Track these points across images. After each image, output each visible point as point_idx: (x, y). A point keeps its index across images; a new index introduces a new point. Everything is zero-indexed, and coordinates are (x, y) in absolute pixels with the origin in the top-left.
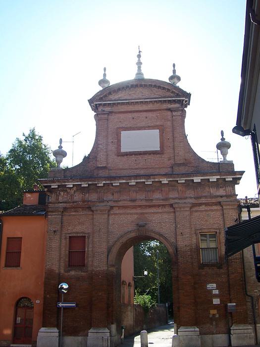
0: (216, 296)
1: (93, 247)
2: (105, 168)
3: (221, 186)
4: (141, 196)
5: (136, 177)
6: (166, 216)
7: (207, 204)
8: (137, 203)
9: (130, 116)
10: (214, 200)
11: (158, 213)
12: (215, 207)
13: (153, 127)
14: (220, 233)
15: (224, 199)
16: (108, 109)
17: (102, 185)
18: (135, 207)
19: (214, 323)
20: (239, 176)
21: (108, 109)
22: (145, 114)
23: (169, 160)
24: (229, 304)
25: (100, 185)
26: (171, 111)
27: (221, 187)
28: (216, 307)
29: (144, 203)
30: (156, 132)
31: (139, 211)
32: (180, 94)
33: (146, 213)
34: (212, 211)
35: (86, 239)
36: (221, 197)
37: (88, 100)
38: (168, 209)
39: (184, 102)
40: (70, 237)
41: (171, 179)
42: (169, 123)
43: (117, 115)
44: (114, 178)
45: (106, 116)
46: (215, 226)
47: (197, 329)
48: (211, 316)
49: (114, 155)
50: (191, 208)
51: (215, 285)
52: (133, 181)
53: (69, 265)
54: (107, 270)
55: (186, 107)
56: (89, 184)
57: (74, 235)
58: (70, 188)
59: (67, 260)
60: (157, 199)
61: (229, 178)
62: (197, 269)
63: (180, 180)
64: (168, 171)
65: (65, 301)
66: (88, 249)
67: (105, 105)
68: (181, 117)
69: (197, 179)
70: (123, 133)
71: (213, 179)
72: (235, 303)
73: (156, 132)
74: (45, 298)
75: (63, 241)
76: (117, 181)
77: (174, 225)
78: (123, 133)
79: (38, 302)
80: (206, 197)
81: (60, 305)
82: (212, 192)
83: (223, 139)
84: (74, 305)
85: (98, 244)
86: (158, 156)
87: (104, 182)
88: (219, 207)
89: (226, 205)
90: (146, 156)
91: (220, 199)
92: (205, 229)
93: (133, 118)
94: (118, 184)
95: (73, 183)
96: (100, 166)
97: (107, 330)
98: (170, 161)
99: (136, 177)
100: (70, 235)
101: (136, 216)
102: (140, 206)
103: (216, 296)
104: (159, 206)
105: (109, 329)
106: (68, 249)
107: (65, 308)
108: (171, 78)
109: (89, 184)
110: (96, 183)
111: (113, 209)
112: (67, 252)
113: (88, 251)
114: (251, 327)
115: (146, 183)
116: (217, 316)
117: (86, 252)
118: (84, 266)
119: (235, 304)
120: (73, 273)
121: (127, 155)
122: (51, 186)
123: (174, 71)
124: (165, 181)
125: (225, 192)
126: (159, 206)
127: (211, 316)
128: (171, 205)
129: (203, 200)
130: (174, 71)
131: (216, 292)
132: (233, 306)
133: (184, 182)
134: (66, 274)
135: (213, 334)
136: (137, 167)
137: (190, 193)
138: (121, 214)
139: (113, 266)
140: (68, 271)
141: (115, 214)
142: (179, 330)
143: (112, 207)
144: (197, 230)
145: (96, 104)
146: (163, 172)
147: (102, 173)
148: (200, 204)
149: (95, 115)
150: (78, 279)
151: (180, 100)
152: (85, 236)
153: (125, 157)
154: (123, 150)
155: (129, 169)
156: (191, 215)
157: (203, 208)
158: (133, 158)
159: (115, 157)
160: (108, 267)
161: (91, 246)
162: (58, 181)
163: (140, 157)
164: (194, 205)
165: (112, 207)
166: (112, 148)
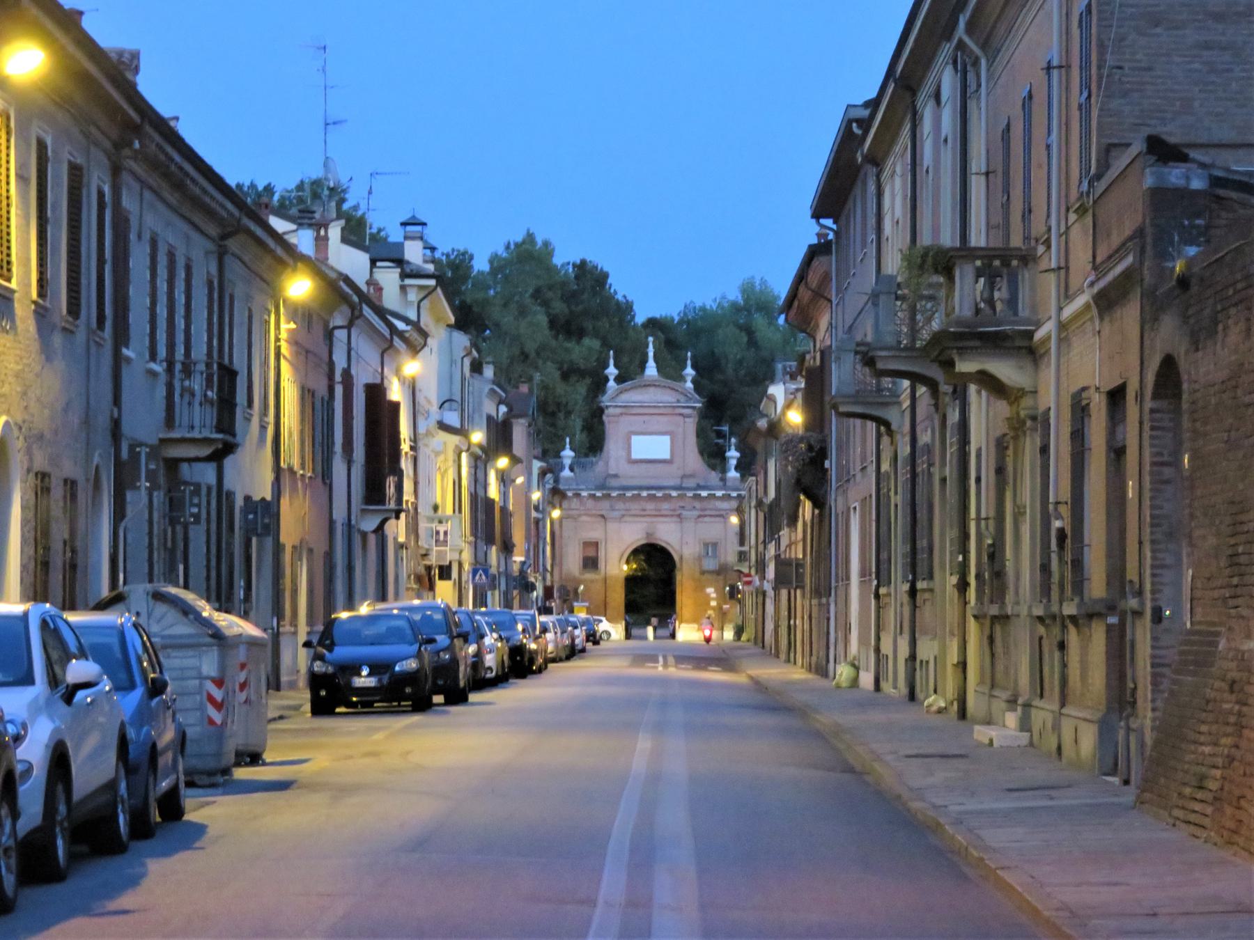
0: (713, 599)
2: (616, 476)
4: (650, 506)
5: (648, 488)
7: (711, 516)
10: (717, 513)
16: (618, 411)
18: (644, 516)
28: (713, 608)
30: (667, 439)
38: (675, 519)
42: (680, 430)
60: (666, 509)
64: (677, 482)
67: (616, 406)
69: (704, 494)
70: (635, 439)
71: (719, 493)
73: (667, 439)
78: (635, 439)
80: (711, 509)
88: (722, 519)
91: (722, 513)
99: (648, 488)
102: (649, 515)
103: (713, 599)
124: (674, 494)
129: (707, 513)
131: (714, 595)
137: (697, 505)
140: (583, 574)
146: (671, 483)
147: (614, 482)
148: (705, 516)
154: (635, 456)
157: (707, 519)
158: (644, 466)
162: (574, 490)
163: (649, 465)
164: (700, 516)
165: (623, 516)
166: (623, 453)
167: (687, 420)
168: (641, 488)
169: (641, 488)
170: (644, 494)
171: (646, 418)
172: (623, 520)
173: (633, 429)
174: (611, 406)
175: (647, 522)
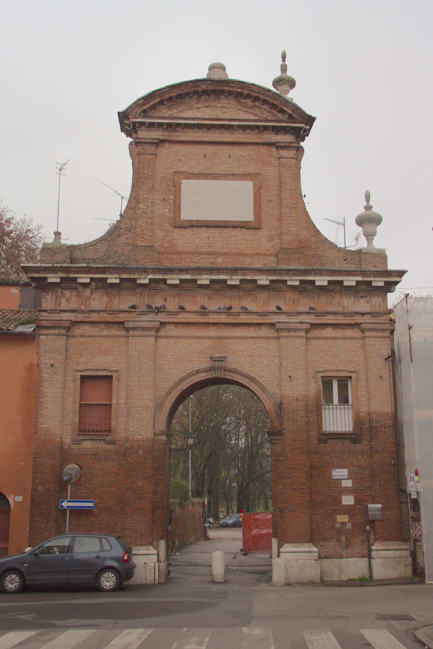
0: (347, 491)
1: (128, 398)
3: (363, 294)
5: (210, 271)
6: (262, 344)
7: (334, 326)
8: (211, 318)
9: (199, 150)
11: (248, 338)
12: (349, 333)
13: (244, 177)
14: (357, 380)
15: (367, 319)
16: (157, 134)
17: (146, 281)
19: (343, 538)
20: (397, 279)
21: (157, 134)
22: (227, 149)
23: (269, 241)
24: (371, 506)
25: (142, 281)
26: (277, 148)
27: (362, 297)
28: (348, 510)
29: (223, 318)
31: (213, 332)
32: (295, 116)
33: (227, 338)
34: (345, 338)
35: (114, 382)
36: (363, 314)
37: (119, 114)
38: (265, 332)
39: (302, 132)
40: (82, 377)
41: (275, 278)
43: (177, 147)
44: (171, 271)
45: (153, 148)
46: (350, 367)
47: (315, 549)
48: (338, 526)
49: (167, 225)
50: (307, 331)
51: (345, 472)
52: (205, 276)
53: (80, 431)
54: (154, 440)
55: (303, 140)
56: (121, 279)
57: (91, 373)
58: (85, 285)
59: (77, 420)
61: (379, 282)
62: (316, 442)
63: (290, 280)
65: (75, 498)
66: (117, 400)
67: (151, 125)
68: (294, 161)
72: (379, 503)
74: (34, 490)
75: (71, 385)
76: (175, 276)
77: (276, 362)
79: (19, 499)
80: (335, 313)
81: (65, 504)
82: (346, 304)
83: (368, 208)
84: (91, 504)
85: (136, 392)
86: (250, 232)
87: (151, 276)
89: (370, 330)
90: (227, 232)
92: (331, 371)
93: (205, 156)
94: (178, 282)
95: (90, 276)
96: (140, 244)
97: (152, 550)
98: (272, 243)
99: (210, 271)
100: (83, 374)
101: (207, 343)
103: (347, 491)
104: (249, 325)
105: (157, 547)
106: (78, 400)
107: (76, 512)
108: (277, 82)
109: (121, 279)
110: (136, 276)
111: (165, 327)
112: (77, 405)
113: (118, 404)
114: (407, 547)
115: (229, 283)
116: (349, 526)
117: (114, 406)
118: (110, 431)
119: (380, 506)
120: (88, 444)
121: (192, 226)
122: (46, 278)
123: (284, 69)
124: (263, 280)
125: (369, 305)
126: (249, 325)
127: (338, 526)
128: (272, 325)
129: (331, 319)
130: (284, 69)
132: (377, 509)
133: (297, 283)
134: (75, 447)
135: (341, 557)
136: (211, 250)
138: (179, 337)
139: (161, 433)
141: (168, 337)
142: (282, 550)
143: (163, 324)
144: (318, 372)
145: (134, 123)
149: (131, 144)
150: (96, 456)
151: (294, 128)
152: (111, 377)
153: (189, 230)
155: (196, 253)
156: (307, 344)
157: (328, 332)
158: (204, 232)
159: (170, 229)
160: (155, 434)
161: (123, 394)
163: (215, 232)
167: (283, 153)
168: (200, 270)
169: (200, 270)
170: (204, 280)
171: (210, 149)
172: (162, 333)
173: (186, 168)
174: (142, 124)
175: (209, 338)
